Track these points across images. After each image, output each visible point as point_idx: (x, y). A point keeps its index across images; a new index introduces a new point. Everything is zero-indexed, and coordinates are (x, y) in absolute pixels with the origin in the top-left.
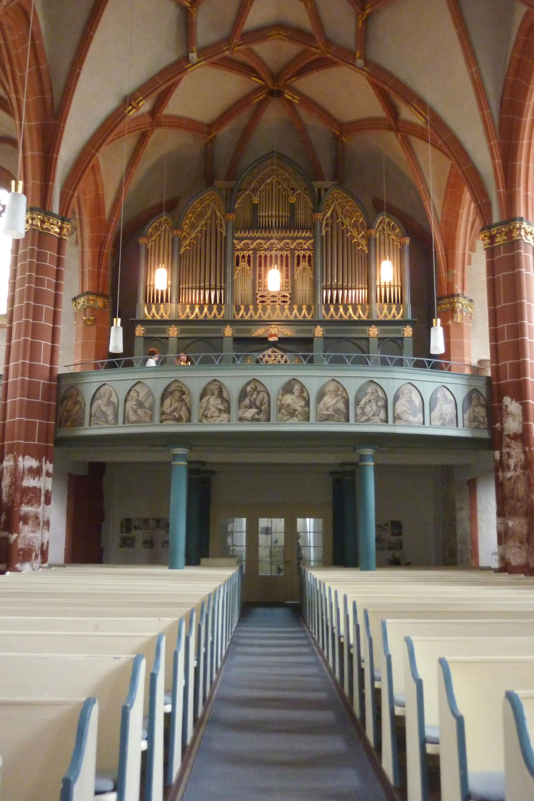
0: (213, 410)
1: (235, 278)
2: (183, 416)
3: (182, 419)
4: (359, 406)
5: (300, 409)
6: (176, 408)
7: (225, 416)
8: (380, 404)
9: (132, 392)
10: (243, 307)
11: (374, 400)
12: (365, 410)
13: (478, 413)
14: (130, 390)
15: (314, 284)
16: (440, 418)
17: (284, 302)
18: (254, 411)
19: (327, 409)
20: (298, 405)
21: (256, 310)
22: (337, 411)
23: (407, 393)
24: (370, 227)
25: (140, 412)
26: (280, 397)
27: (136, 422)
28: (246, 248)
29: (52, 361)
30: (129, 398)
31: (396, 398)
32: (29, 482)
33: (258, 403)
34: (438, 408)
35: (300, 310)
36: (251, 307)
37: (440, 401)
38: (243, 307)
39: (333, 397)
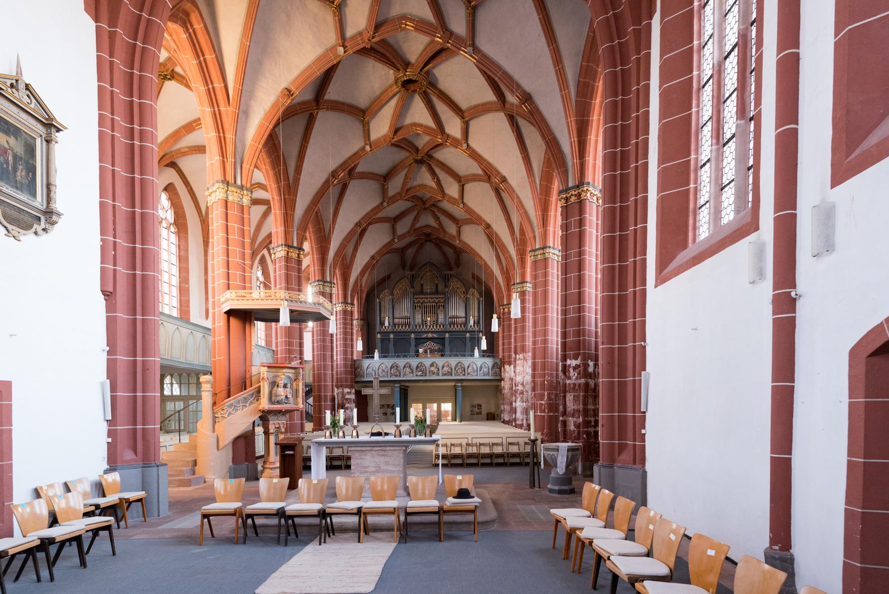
15: (445, 316)
24: (467, 293)
28: (419, 302)
29: (352, 355)
32: (348, 397)
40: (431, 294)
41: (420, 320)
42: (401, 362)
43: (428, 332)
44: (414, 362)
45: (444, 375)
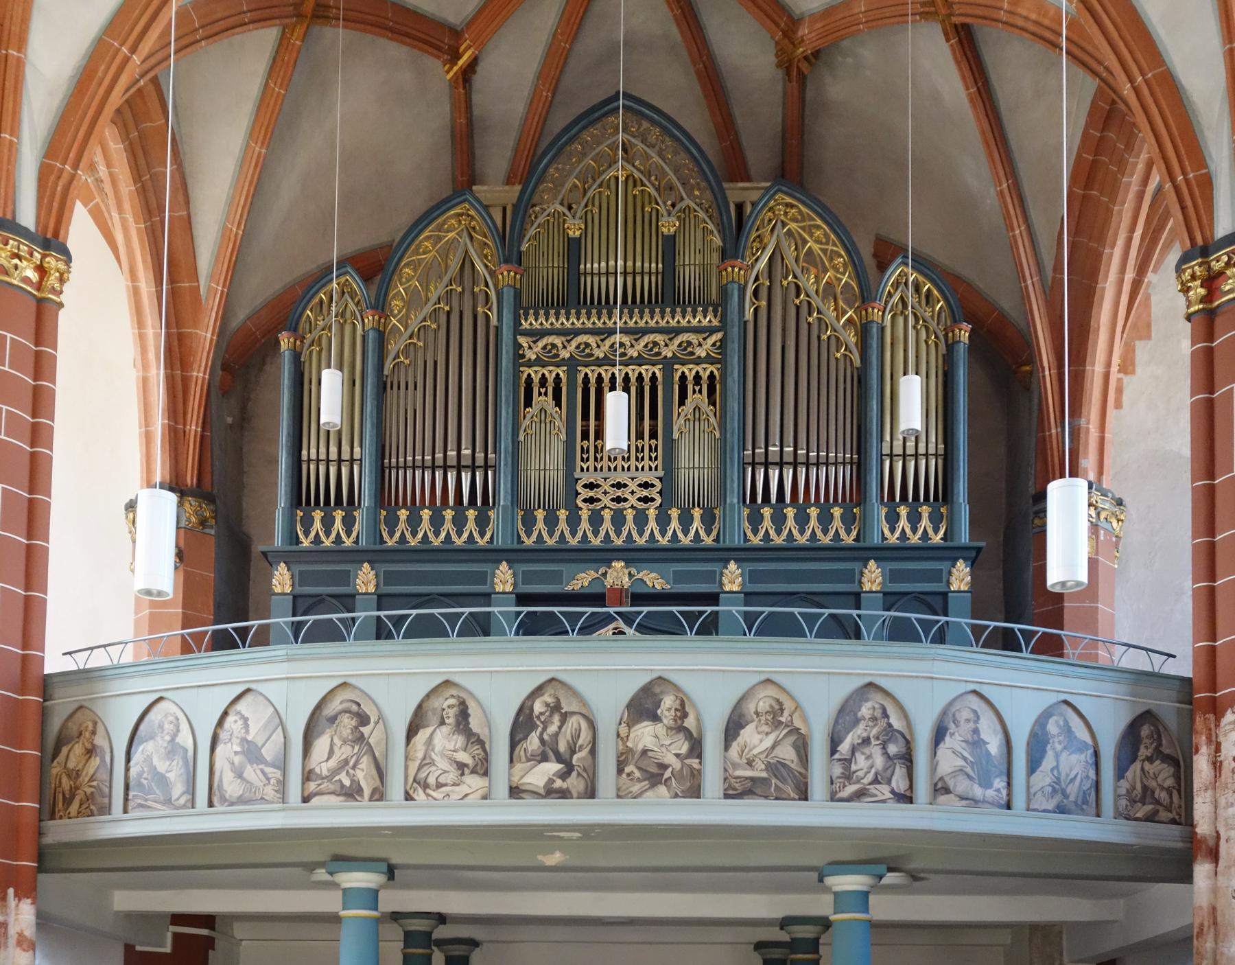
0: (442, 768)
1: (521, 437)
2: (363, 784)
3: (360, 790)
4: (837, 756)
5: (676, 764)
6: (346, 762)
7: (474, 783)
8: (893, 749)
9: (230, 719)
10: (540, 514)
11: (877, 738)
12: (854, 767)
13: (1156, 777)
14: (225, 713)
16: (1054, 791)
17: (645, 500)
18: (553, 767)
19: (750, 763)
20: (671, 751)
21: (574, 522)
22: (777, 768)
23: (968, 720)
25: (251, 773)
26: (623, 730)
27: (241, 800)
30: (223, 735)
31: (939, 734)
33: (562, 747)
34: (1048, 762)
35: (686, 521)
36: (563, 514)
37: (1056, 744)
38: (540, 514)
39: (766, 729)
40: (631, 303)
41: (557, 476)
42: (393, 675)
43: (605, 555)
44: (499, 673)
45: (738, 790)
